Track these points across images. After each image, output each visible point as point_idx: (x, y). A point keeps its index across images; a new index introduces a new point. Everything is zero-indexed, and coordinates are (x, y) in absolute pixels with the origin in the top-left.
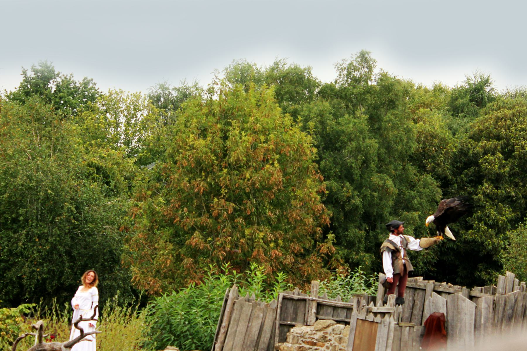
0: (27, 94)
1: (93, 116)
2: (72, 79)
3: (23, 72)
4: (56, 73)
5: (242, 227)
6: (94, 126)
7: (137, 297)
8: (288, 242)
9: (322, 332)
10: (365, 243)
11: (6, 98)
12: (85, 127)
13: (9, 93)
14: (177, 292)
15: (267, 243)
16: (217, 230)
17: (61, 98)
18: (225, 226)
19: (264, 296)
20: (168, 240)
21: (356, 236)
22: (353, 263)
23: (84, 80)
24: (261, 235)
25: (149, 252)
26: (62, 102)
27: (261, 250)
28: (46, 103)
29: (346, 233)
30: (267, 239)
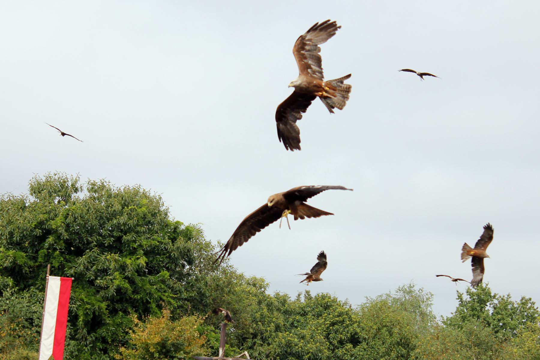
0: (464, 319)
1: (534, 337)
2: (509, 300)
3: (459, 296)
4: (492, 295)
6: (536, 347)
11: (442, 324)
12: (526, 349)
13: (445, 318)
17: (499, 320)
23: (522, 300)
26: (501, 324)
28: (485, 326)
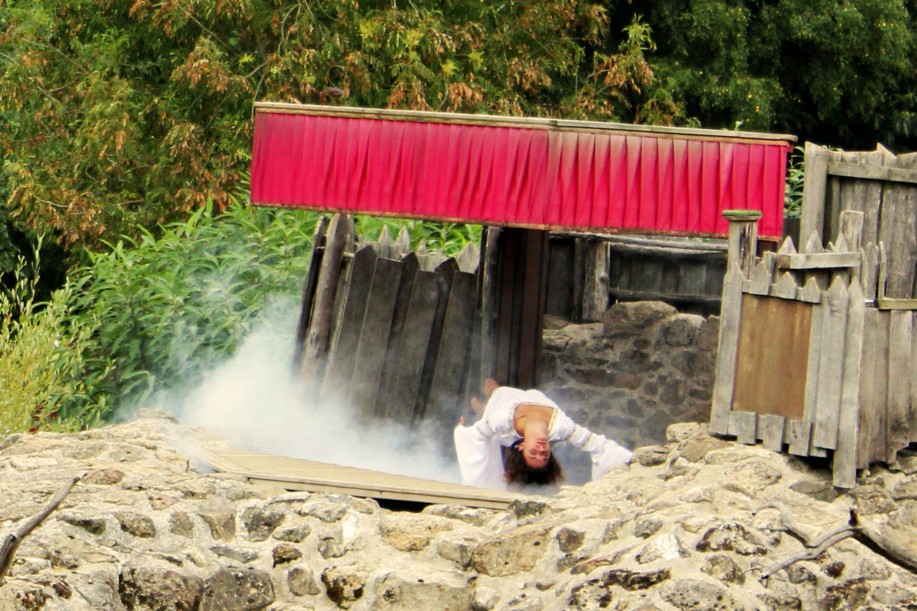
5: (350, 16)
7: (30, 257)
8: (499, 54)
9: (631, 340)
10: (749, 44)
14: (157, 233)
15: (431, 61)
16: (268, 30)
18: (294, 13)
19: (437, 235)
20: (117, 70)
21: (717, 25)
22: (712, 109)
24: (413, 37)
25: (61, 109)
27: (417, 85)
29: (687, 16)
30: (433, 49)
